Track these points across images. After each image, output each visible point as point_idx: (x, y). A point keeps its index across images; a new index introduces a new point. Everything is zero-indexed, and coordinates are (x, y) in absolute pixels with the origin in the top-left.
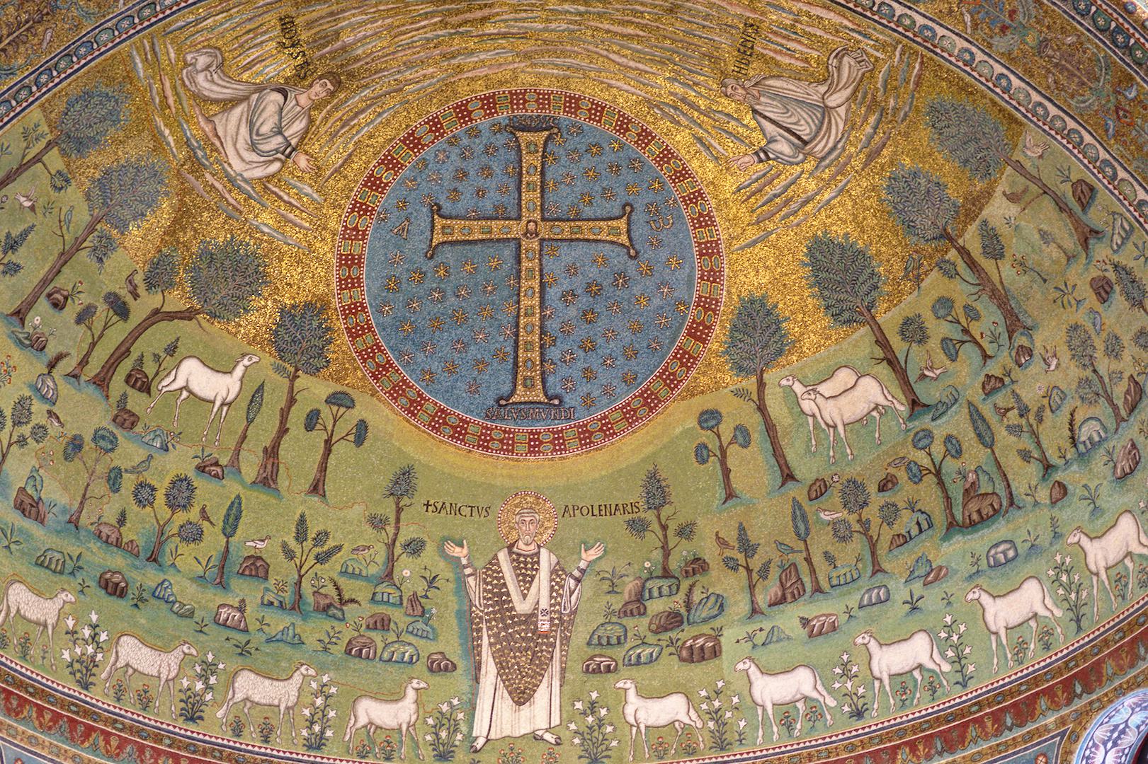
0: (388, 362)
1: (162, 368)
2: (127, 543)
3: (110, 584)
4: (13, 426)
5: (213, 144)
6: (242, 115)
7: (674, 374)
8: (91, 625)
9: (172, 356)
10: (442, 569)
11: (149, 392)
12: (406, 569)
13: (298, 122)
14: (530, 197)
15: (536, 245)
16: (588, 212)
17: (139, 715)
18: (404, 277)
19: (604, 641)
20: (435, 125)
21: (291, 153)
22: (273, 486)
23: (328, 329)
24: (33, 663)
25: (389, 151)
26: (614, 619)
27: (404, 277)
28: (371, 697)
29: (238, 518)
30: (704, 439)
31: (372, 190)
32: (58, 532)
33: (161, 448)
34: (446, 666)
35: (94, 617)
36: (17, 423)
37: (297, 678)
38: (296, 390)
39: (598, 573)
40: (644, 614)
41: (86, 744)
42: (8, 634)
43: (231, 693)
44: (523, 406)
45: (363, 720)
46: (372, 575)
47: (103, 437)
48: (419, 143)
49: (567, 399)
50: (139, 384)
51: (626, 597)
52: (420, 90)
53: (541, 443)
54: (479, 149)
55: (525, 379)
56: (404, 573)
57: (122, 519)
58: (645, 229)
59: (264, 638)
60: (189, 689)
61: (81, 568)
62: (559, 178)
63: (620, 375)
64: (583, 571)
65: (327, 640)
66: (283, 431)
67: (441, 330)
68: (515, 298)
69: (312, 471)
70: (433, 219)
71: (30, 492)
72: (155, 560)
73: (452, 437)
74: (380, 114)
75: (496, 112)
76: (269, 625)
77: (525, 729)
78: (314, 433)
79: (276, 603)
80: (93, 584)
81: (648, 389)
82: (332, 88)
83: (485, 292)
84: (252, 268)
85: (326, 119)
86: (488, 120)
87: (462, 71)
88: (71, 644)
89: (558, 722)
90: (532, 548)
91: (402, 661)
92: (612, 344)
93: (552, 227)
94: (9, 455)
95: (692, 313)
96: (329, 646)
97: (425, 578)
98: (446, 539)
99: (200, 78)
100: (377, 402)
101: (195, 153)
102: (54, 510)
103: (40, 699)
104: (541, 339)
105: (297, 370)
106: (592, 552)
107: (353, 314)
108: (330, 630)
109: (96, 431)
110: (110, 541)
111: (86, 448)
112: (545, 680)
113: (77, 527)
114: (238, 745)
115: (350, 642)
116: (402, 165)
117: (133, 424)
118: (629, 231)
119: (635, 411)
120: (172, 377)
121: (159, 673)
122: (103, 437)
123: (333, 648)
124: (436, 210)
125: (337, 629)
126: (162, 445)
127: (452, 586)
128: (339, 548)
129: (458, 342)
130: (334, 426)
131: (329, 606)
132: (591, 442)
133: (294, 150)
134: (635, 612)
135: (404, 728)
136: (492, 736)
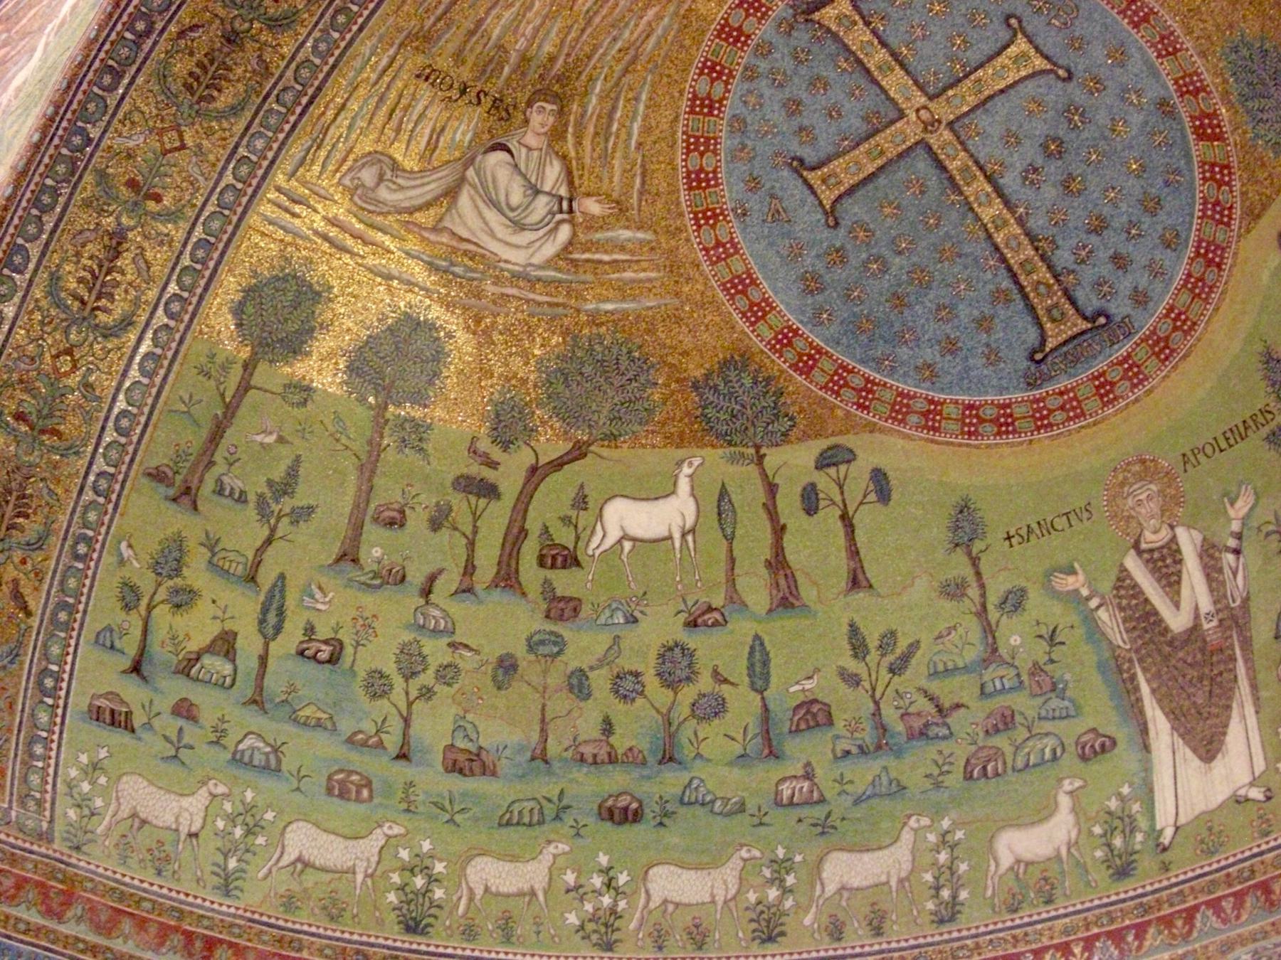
0: (868, 380)
1: (579, 531)
2: (625, 754)
3: (617, 812)
4: (407, 681)
5: (465, 252)
7: (1217, 203)
8: (601, 871)
9: (586, 509)
10: (1058, 614)
11: (577, 563)
12: (1014, 636)
13: (548, 169)
14: (895, 82)
15: (947, 135)
16: (973, 56)
20: (713, 70)
21: (570, 206)
22: (797, 603)
23: (768, 380)
25: (684, 133)
27: (820, 266)
28: (1011, 826)
29: (766, 663)
33: (627, 622)
34: (1103, 746)
35: (603, 860)
36: (409, 675)
37: (907, 836)
38: (770, 474)
42: (477, 922)
43: (818, 887)
44: (1065, 349)
45: (1006, 861)
47: (542, 642)
49: (1112, 308)
50: (560, 559)
52: (658, 43)
53: (1112, 384)
54: (788, 64)
55: (1049, 310)
56: (1012, 642)
57: (608, 727)
58: (1053, 33)
59: (850, 799)
60: (759, 903)
61: (569, 807)
62: (906, 36)
64: (1239, 536)
65: (936, 772)
67: (910, 306)
68: (970, 215)
69: (839, 562)
70: (805, 181)
72: (671, 759)
73: (999, 433)
74: (637, 99)
76: (851, 782)
77: (1221, 794)
78: (821, 514)
79: (854, 750)
80: (591, 820)
81: (1200, 241)
82: (555, 107)
83: (929, 229)
85: (579, 143)
88: (576, 903)
90: (1165, 534)
91: (1042, 762)
92: (1124, 207)
93: (948, 100)
94: (414, 717)
95: (1184, 110)
96: (940, 779)
97: (1040, 636)
98: (1049, 574)
99: (384, 193)
101: (453, 273)
102: (508, 752)
104: (1037, 249)
105: (757, 448)
106: (1239, 504)
107: (786, 345)
108: (936, 757)
109: (529, 640)
111: (523, 664)
112: (1235, 713)
113: (546, 762)
115: (968, 761)
116: (715, 139)
117: (576, 611)
118: (1037, 49)
119: (1201, 279)
120: (599, 533)
121: (713, 896)
122: (542, 642)
124: (799, 166)
125: (946, 752)
127: (1080, 632)
128: (915, 646)
130: (842, 493)
131: (927, 725)
132: (1173, 351)
133: (570, 201)
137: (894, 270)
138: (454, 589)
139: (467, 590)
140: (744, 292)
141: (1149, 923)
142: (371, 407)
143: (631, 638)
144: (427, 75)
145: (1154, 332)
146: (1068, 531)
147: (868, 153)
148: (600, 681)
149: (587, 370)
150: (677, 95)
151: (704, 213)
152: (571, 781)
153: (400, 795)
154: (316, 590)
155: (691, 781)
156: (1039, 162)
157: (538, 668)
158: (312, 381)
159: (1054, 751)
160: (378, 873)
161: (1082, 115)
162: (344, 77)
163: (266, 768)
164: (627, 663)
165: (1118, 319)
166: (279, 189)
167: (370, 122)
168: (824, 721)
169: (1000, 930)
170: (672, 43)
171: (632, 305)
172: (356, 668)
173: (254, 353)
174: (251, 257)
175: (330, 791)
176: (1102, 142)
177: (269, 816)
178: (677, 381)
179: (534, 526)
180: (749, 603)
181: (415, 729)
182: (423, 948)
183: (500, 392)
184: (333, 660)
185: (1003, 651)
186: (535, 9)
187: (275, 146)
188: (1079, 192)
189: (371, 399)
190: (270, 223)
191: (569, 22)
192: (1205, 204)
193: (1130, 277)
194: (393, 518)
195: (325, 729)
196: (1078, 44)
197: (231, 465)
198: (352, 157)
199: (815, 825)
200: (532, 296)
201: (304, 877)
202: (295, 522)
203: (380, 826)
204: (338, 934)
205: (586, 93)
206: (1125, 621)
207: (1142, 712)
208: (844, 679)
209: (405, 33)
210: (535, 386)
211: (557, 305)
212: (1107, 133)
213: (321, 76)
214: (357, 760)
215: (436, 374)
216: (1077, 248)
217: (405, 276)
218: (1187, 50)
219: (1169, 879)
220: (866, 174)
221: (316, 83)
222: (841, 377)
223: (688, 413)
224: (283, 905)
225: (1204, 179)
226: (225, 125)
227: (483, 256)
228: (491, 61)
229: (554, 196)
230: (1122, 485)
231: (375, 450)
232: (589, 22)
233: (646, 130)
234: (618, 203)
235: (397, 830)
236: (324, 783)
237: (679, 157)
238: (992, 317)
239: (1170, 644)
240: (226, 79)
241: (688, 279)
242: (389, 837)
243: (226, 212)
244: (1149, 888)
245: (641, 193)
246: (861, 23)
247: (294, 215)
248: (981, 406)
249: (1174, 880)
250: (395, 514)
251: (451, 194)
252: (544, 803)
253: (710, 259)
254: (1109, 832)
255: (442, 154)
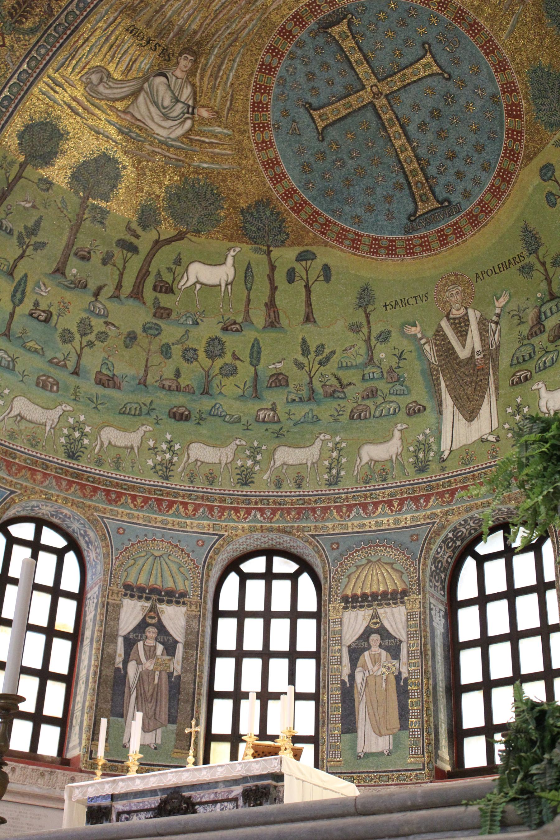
0: (327, 220)
1: (176, 275)
2: (185, 388)
3: (177, 415)
4: (81, 337)
6: (145, 99)
10: (406, 345)
13: (185, 90)
14: (363, 70)
15: (384, 101)
16: (404, 61)
17: (207, 489)
18: (312, 160)
19: (521, 361)
20: (274, 51)
22: (278, 326)
23: (278, 214)
24: (125, 471)
25: (255, 82)
26: (526, 342)
27: (312, 160)
28: (371, 443)
29: (259, 353)
30: (549, 189)
31: (260, 112)
32: (133, 392)
33: (193, 324)
34: (419, 410)
35: (169, 437)
37: (318, 443)
38: (273, 260)
39: (509, 313)
40: (544, 331)
41: (171, 512)
42: (103, 458)
43: (272, 462)
44: (426, 216)
45: (365, 459)
46: (360, 364)
47: (150, 328)
48: (271, 68)
50: (164, 289)
51: (530, 322)
52: (249, 33)
53: (447, 236)
54: (311, 53)
55: (421, 196)
57: (178, 374)
58: (445, 55)
60: (242, 466)
61: (153, 409)
63: (480, 167)
64: (499, 316)
65: (336, 414)
66: (274, 289)
67: (353, 186)
68: (389, 143)
69: (302, 308)
70: (311, 115)
71: (105, 373)
72: (207, 393)
73: (388, 254)
74: (234, 60)
75: (306, 23)
76: (294, 414)
77: (475, 437)
78: (295, 283)
79: (297, 399)
80: (165, 417)
81: (500, 169)
82: (192, 58)
84: (209, 192)
85: (202, 79)
86: (304, 31)
87: (267, 7)
88: (153, 456)
89: (497, 426)
90: (462, 311)
92: (465, 148)
94: (83, 355)
96: (338, 417)
97: (395, 355)
98: (403, 325)
99: (101, 88)
100: (330, 249)
101: (130, 136)
102: (127, 379)
103: (133, 491)
104: (419, 164)
105: (269, 247)
106: (501, 300)
108: (337, 407)
109: (144, 326)
110: (171, 389)
111: (139, 337)
113: (146, 386)
114: (279, 494)
115: (352, 411)
116: (270, 87)
117: (169, 315)
118: (436, 61)
121: (220, 460)
122: (150, 328)
123: (341, 418)
124: (309, 107)
125: (342, 405)
126: (193, 322)
127: (414, 354)
128: (333, 353)
129: (367, 189)
130: (307, 275)
131: (334, 391)
132: (479, 222)
133: (194, 108)
134: (538, 332)
135: (394, 458)
136: (454, 448)
137: (348, 167)
138: (110, 295)
139: (116, 297)
140: (273, 168)
141: (433, 494)
142: (80, 197)
143: (194, 332)
144: (131, 30)
145: (471, 212)
146: (415, 305)
147: (344, 105)
148: (177, 350)
149: (190, 196)
150: (254, 61)
151: (259, 124)
152: (157, 397)
153: (72, 391)
154: (42, 285)
155: (216, 405)
156: (427, 120)
157: (147, 340)
158: (53, 179)
159: (395, 410)
160: (58, 427)
161: (452, 99)
162: (89, 23)
163: (8, 368)
164: (191, 344)
165: (454, 204)
166: (49, 77)
167: (99, 51)
168: (284, 384)
169: (359, 491)
170: (255, 34)
171: (217, 166)
172: (57, 326)
173: (26, 159)
174: (31, 109)
175: (37, 384)
176: (460, 114)
177: (7, 391)
178: (234, 208)
179: (153, 269)
180: (255, 323)
181: (83, 361)
182: (76, 466)
183: (145, 201)
184: (47, 321)
185: (376, 360)
186: (191, 4)
187: (51, 54)
188: (445, 137)
189: (81, 194)
190: (43, 94)
191: (207, 14)
192: (506, 150)
193: (463, 183)
194: (85, 255)
195: (39, 353)
196: (456, 62)
197: (7, 215)
198: (88, 67)
199: (273, 433)
200: (167, 154)
201: (20, 424)
202: (35, 249)
203: (60, 405)
204: (34, 454)
205: (210, 54)
206: (437, 351)
207: (440, 395)
208: (296, 365)
209: (124, 6)
210: (163, 200)
211: (180, 160)
212: (464, 109)
213: (79, 21)
214: (53, 372)
215: (115, 186)
216: (440, 166)
217: (106, 133)
218: (511, 69)
219: (444, 475)
220: (341, 116)
221: (76, 24)
222: (314, 217)
223: (236, 224)
224: (9, 435)
225: (508, 137)
226: (27, 38)
227: (146, 130)
228: (164, 28)
229: (186, 104)
230: (445, 286)
231: (80, 220)
232: (216, 17)
233: (237, 77)
234: (217, 113)
235: (69, 408)
236: (35, 379)
237: (251, 93)
238: (393, 196)
239: (458, 364)
240: (30, 13)
241: (246, 157)
242: (64, 411)
243: (22, 84)
244: (434, 478)
245: (229, 110)
246: (351, 37)
247: (55, 92)
248: (381, 239)
249: (446, 475)
250: (86, 253)
251: (135, 94)
252: (142, 405)
253: (258, 149)
254: (417, 451)
255: (133, 74)
